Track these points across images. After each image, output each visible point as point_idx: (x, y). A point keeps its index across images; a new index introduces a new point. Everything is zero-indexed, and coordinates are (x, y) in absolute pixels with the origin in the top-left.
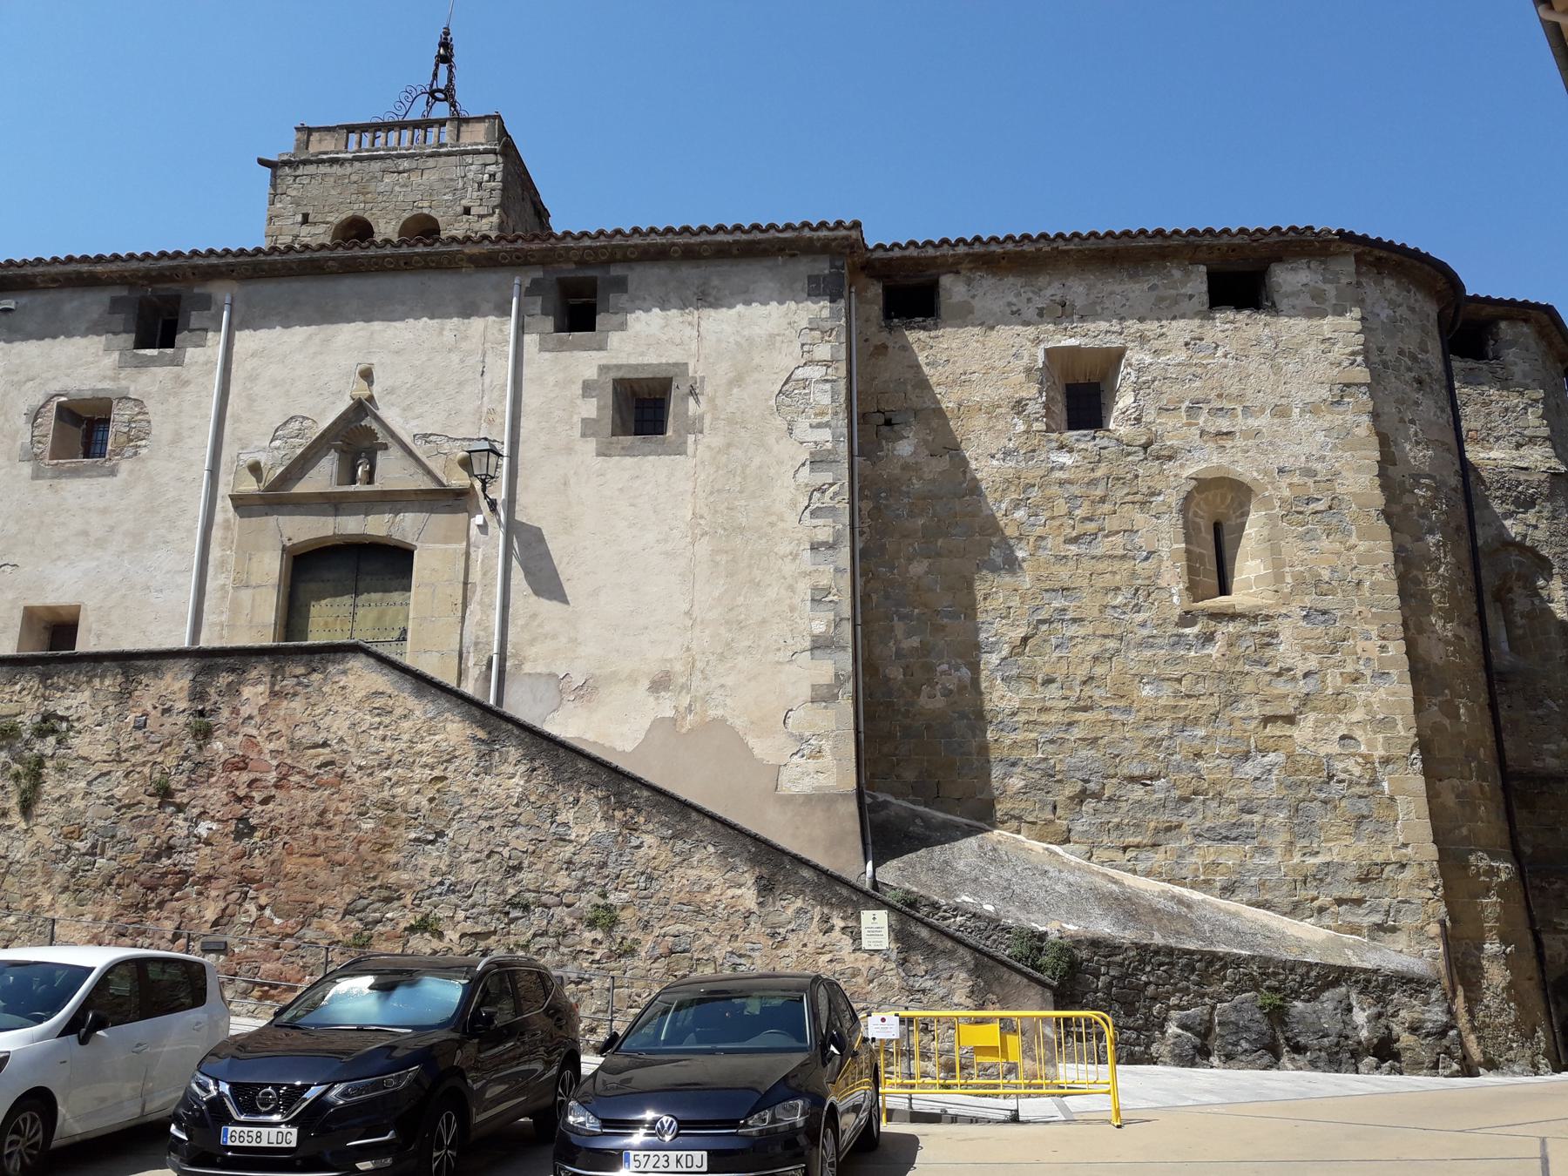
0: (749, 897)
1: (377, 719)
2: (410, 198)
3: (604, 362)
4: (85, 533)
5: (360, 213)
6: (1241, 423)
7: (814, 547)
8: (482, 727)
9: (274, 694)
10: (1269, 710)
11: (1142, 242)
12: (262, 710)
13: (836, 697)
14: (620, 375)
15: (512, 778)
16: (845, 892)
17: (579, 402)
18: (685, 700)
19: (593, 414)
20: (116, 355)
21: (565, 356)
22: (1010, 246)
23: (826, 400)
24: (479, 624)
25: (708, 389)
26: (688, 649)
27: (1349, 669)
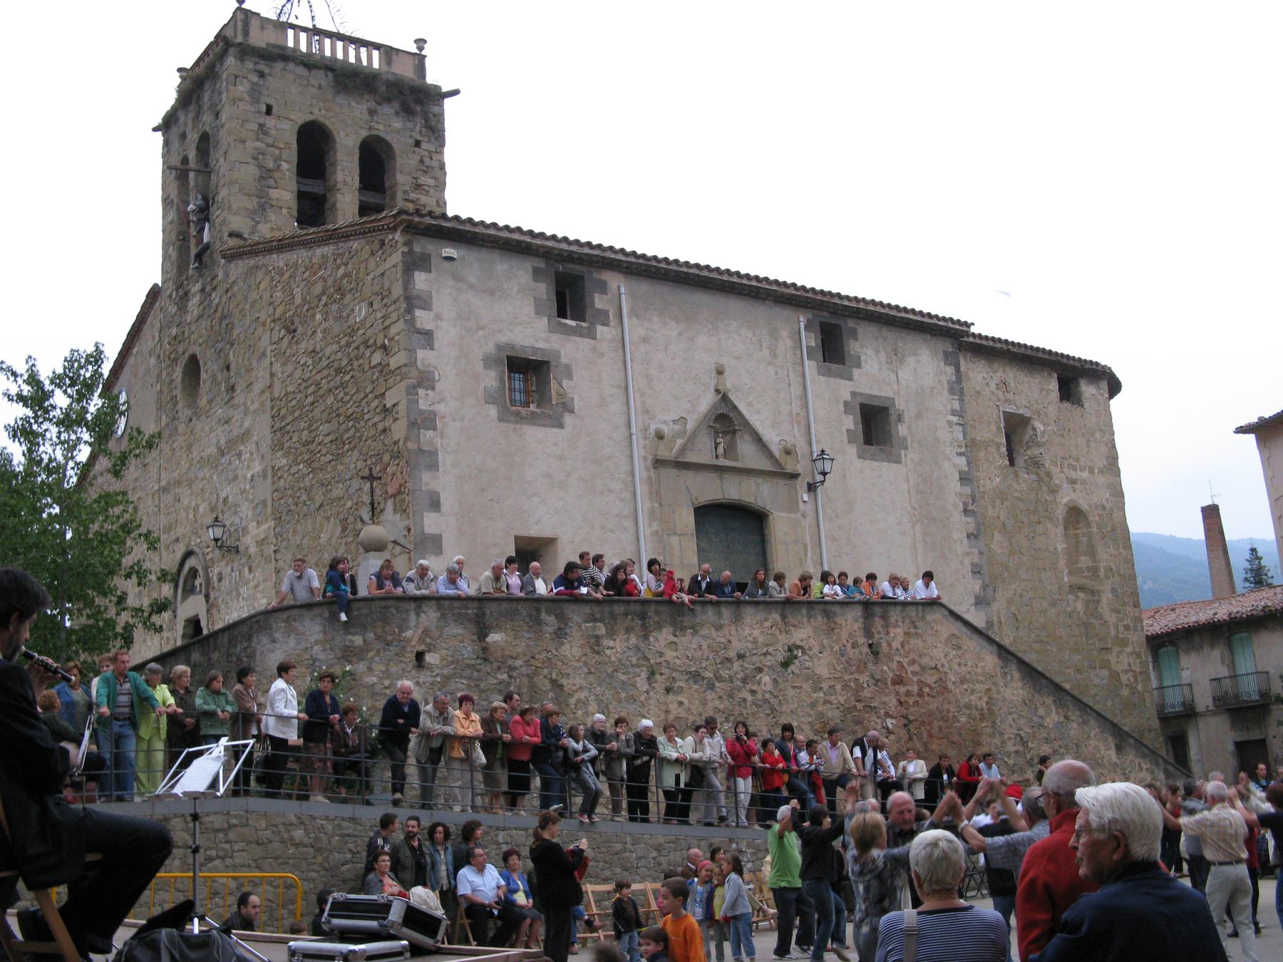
0: (1112, 753)
5: (322, 120)
7: (968, 537)
15: (1014, 690)
19: (852, 427)
20: (545, 319)
23: (961, 437)
25: (906, 419)
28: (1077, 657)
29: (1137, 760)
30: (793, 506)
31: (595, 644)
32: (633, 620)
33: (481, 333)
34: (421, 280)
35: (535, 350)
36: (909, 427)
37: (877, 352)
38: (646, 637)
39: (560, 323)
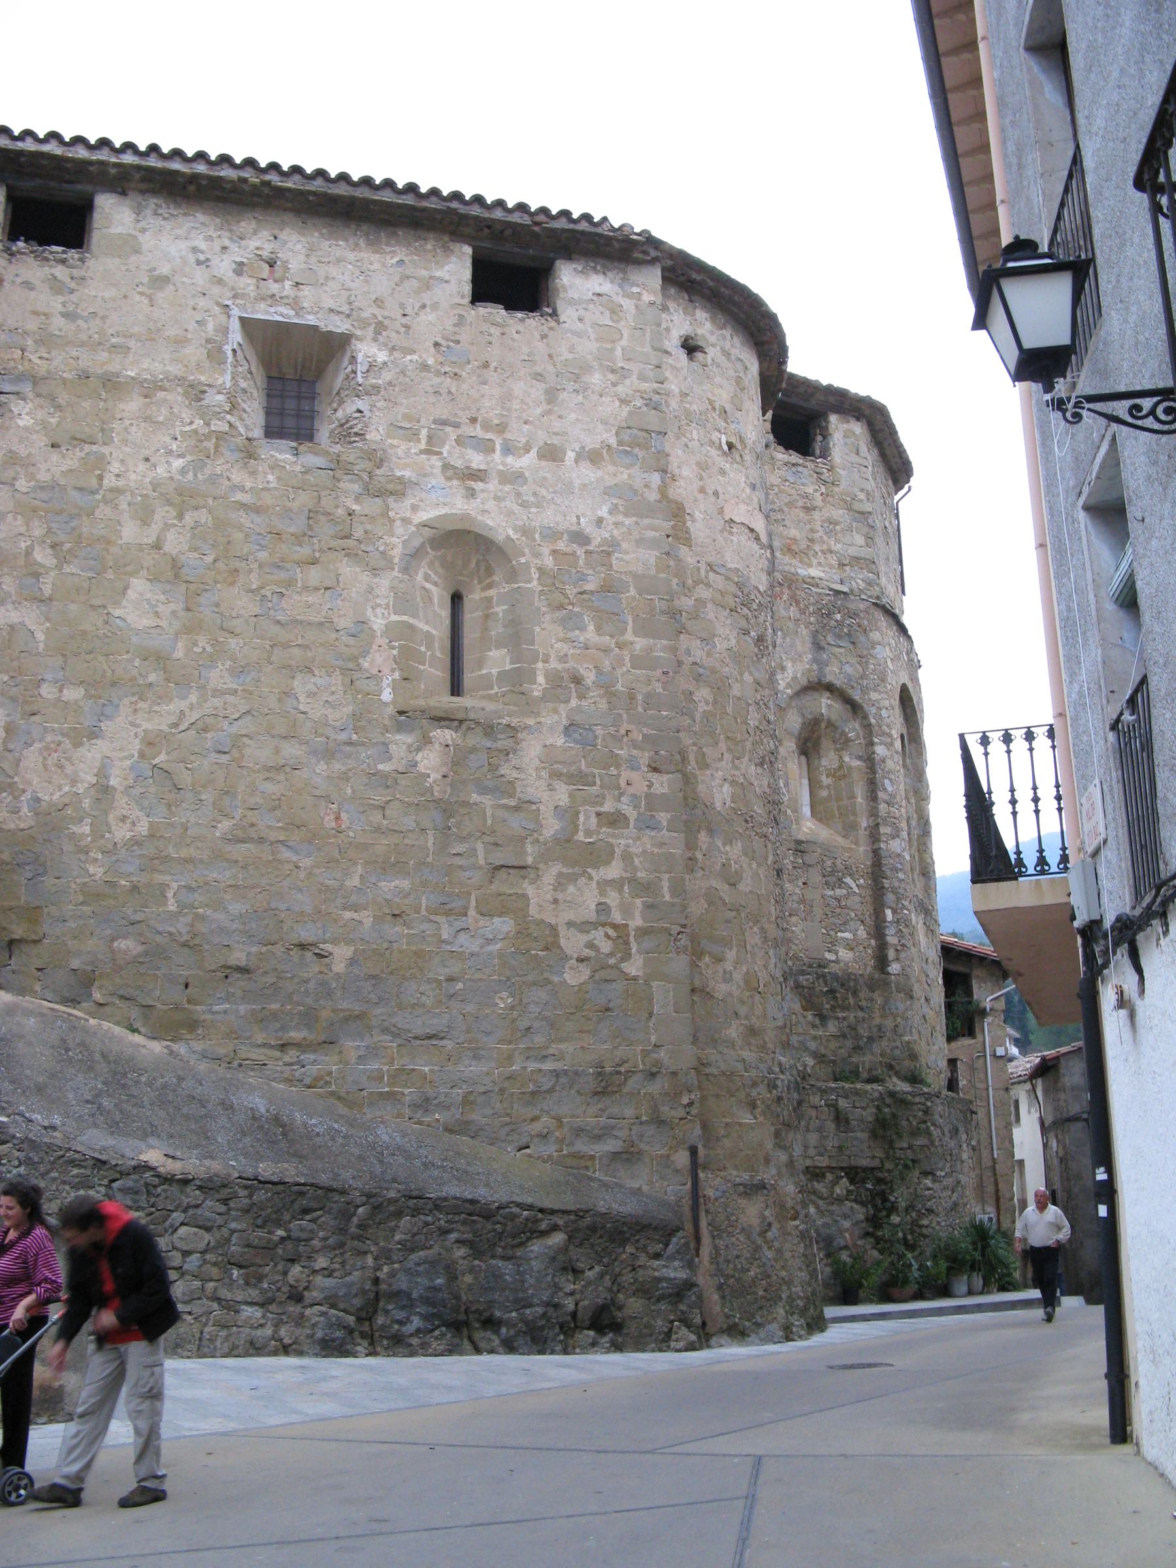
10: (499, 858)
11: (387, 196)
22: (201, 168)
27: (608, 807)
28: (392, 886)
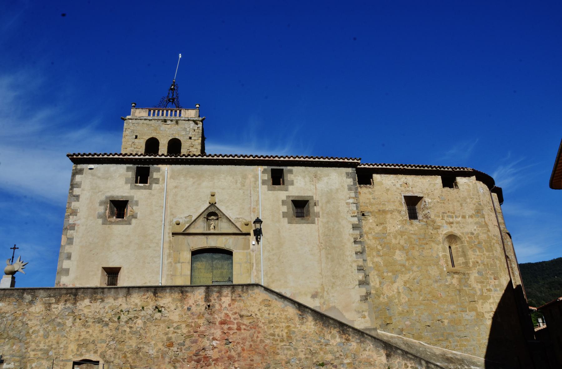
0: (384, 359)
1: (266, 308)
2: (172, 133)
3: (288, 195)
4: (121, 243)
6: (455, 220)
7: (356, 253)
8: (299, 310)
9: (232, 300)
10: (471, 299)
12: (230, 305)
13: (367, 299)
14: (293, 199)
15: (310, 325)
16: (410, 356)
17: (281, 206)
18: (322, 301)
20: (129, 185)
21: (276, 192)
23: (355, 209)
24: (256, 276)
25: (320, 204)
26: (322, 285)
27: (488, 288)
28: (453, 307)
29: (403, 362)
30: (247, 246)
31: (48, 306)
32: (70, 296)
33: (100, 193)
34: (78, 178)
35: (123, 197)
36: (322, 208)
37: (304, 177)
38: (75, 303)
39: (135, 186)
